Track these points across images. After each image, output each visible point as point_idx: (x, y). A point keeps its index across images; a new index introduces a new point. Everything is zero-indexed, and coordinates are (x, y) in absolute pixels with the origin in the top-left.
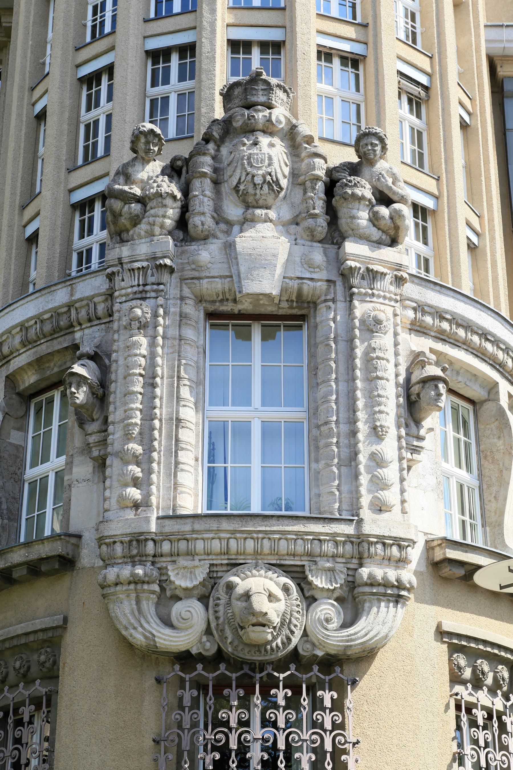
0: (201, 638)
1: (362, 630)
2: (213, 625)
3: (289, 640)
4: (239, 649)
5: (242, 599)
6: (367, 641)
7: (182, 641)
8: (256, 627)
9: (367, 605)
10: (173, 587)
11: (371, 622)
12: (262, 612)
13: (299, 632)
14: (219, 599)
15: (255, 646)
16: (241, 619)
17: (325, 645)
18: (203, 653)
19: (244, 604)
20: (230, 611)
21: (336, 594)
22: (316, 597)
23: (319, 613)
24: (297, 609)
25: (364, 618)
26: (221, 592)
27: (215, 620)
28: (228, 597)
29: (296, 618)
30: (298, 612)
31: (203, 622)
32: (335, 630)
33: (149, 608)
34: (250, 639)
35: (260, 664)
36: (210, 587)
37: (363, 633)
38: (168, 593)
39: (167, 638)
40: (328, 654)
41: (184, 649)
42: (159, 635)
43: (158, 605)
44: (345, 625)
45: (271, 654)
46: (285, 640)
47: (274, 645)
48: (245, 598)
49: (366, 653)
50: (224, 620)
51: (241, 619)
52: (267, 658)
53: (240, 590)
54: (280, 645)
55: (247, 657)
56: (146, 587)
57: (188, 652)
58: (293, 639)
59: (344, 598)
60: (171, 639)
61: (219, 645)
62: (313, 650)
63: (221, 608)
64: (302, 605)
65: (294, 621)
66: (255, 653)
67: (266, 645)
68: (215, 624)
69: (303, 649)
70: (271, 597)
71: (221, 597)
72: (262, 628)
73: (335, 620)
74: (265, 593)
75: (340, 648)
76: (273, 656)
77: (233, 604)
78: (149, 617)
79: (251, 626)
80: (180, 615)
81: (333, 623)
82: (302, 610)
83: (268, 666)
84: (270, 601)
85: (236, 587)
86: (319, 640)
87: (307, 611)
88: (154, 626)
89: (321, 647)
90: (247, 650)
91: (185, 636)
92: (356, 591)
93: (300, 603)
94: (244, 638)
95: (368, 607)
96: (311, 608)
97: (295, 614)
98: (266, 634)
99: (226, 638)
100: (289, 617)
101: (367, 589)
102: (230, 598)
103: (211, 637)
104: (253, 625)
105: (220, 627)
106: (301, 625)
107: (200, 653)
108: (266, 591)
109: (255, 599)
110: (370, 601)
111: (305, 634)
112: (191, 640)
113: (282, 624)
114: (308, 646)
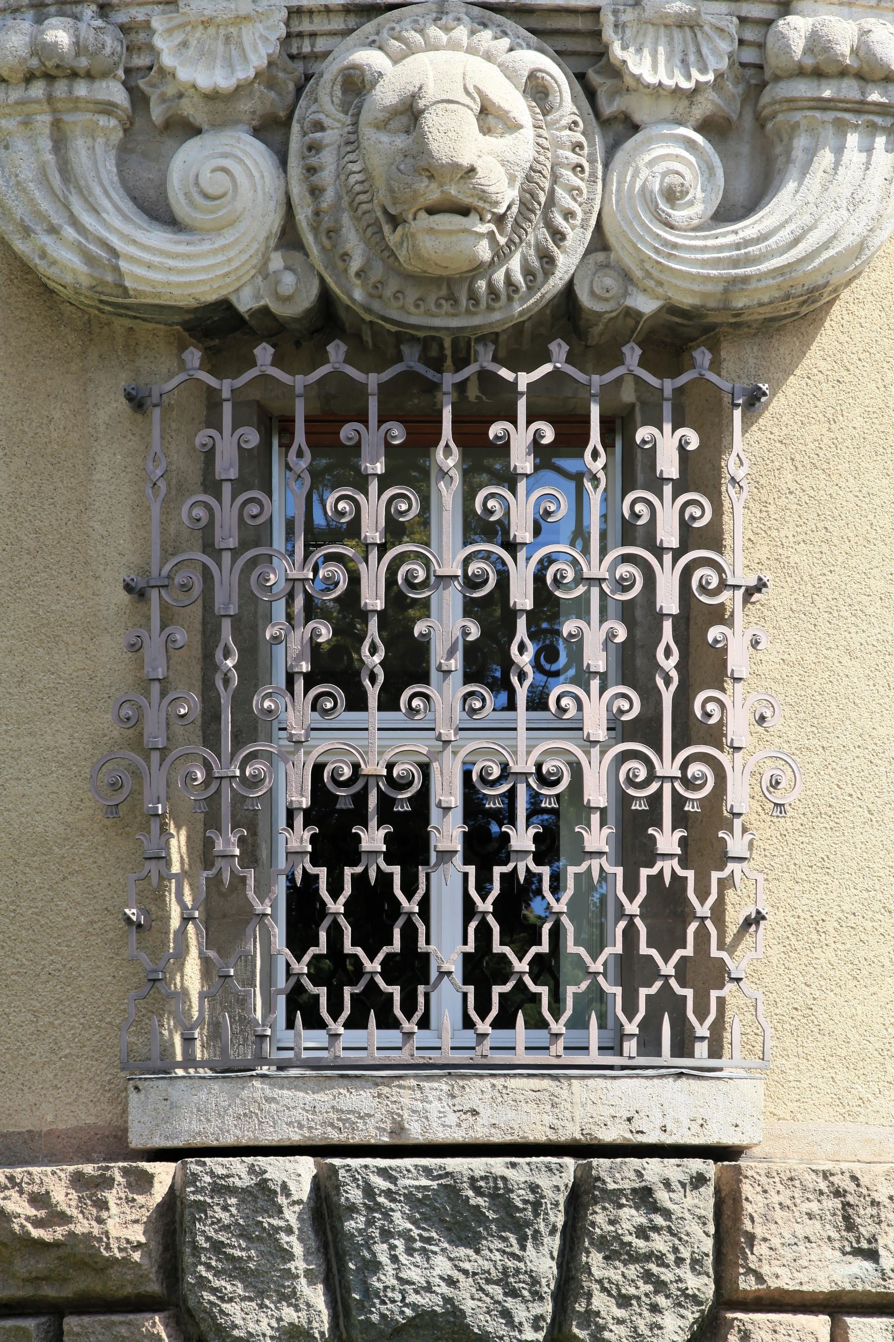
0: (266, 261)
1: (782, 226)
2: (303, 215)
3: (547, 260)
4: (388, 292)
5: (394, 124)
6: (800, 261)
7: (204, 269)
8: (437, 217)
9: (801, 142)
10: (170, 90)
11: (811, 199)
12: (456, 166)
13: (578, 239)
14: (319, 127)
15: (437, 281)
16: (391, 191)
17: (662, 277)
18: (276, 308)
19: (401, 141)
20: (356, 167)
21: (703, 108)
22: (637, 117)
23: (644, 173)
24: (574, 158)
25: (791, 185)
26: (326, 103)
27: (308, 199)
28: (348, 120)
29: (573, 190)
30: (578, 168)
31: (272, 204)
32: (695, 229)
33: (95, 163)
34: (419, 257)
35: (455, 343)
36: (291, 87)
37: (784, 235)
38: (157, 113)
39: (156, 259)
40: (672, 309)
41: (212, 297)
42: (132, 250)
43: (124, 151)
44: (726, 214)
45: (490, 309)
46: (535, 263)
47: (499, 277)
48: (404, 119)
49: (794, 302)
50: (339, 198)
51: (391, 191)
52: (476, 321)
53: (386, 95)
54: (518, 277)
55: (413, 320)
56: (81, 89)
57: (225, 306)
58: (561, 259)
59: (728, 120)
60: (171, 263)
61: (322, 280)
62: (626, 294)
63: (328, 159)
64: (592, 144)
65: (564, 198)
66: (439, 306)
67: (473, 280)
68: (309, 211)
69: (592, 293)
70: (488, 116)
71: (327, 122)
72: (458, 219)
73: (697, 192)
74: (467, 100)
75: (709, 288)
76: (496, 316)
77: (365, 143)
78: (97, 190)
79: (423, 215)
80: (197, 184)
81: (691, 203)
82: (592, 161)
83: (480, 349)
84: (486, 130)
85: (374, 84)
86: (642, 260)
87: (606, 166)
88: (116, 221)
89: (652, 283)
90: (412, 295)
91: (215, 252)
92: (765, 98)
93: (582, 139)
94: (402, 255)
95: (806, 150)
96: (620, 156)
97: (567, 174)
98: (472, 238)
99: (345, 257)
100: (546, 185)
101: (803, 89)
102: (355, 124)
103: (298, 256)
104: (431, 211)
105: (327, 222)
106: (588, 213)
107: (265, 311)
108: (470, 95)
109: (434, 122)
110: (811, 130)
111: (600, 242)
112: (235, 264)
113: (526, 208)
114: (610, 281)
